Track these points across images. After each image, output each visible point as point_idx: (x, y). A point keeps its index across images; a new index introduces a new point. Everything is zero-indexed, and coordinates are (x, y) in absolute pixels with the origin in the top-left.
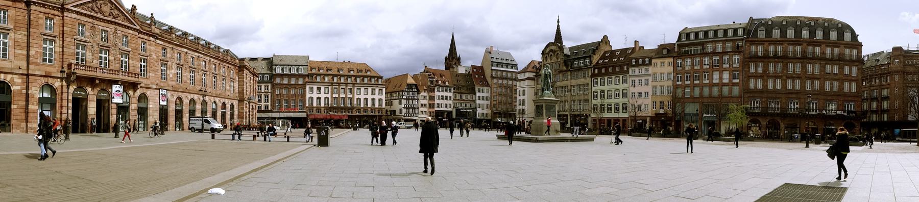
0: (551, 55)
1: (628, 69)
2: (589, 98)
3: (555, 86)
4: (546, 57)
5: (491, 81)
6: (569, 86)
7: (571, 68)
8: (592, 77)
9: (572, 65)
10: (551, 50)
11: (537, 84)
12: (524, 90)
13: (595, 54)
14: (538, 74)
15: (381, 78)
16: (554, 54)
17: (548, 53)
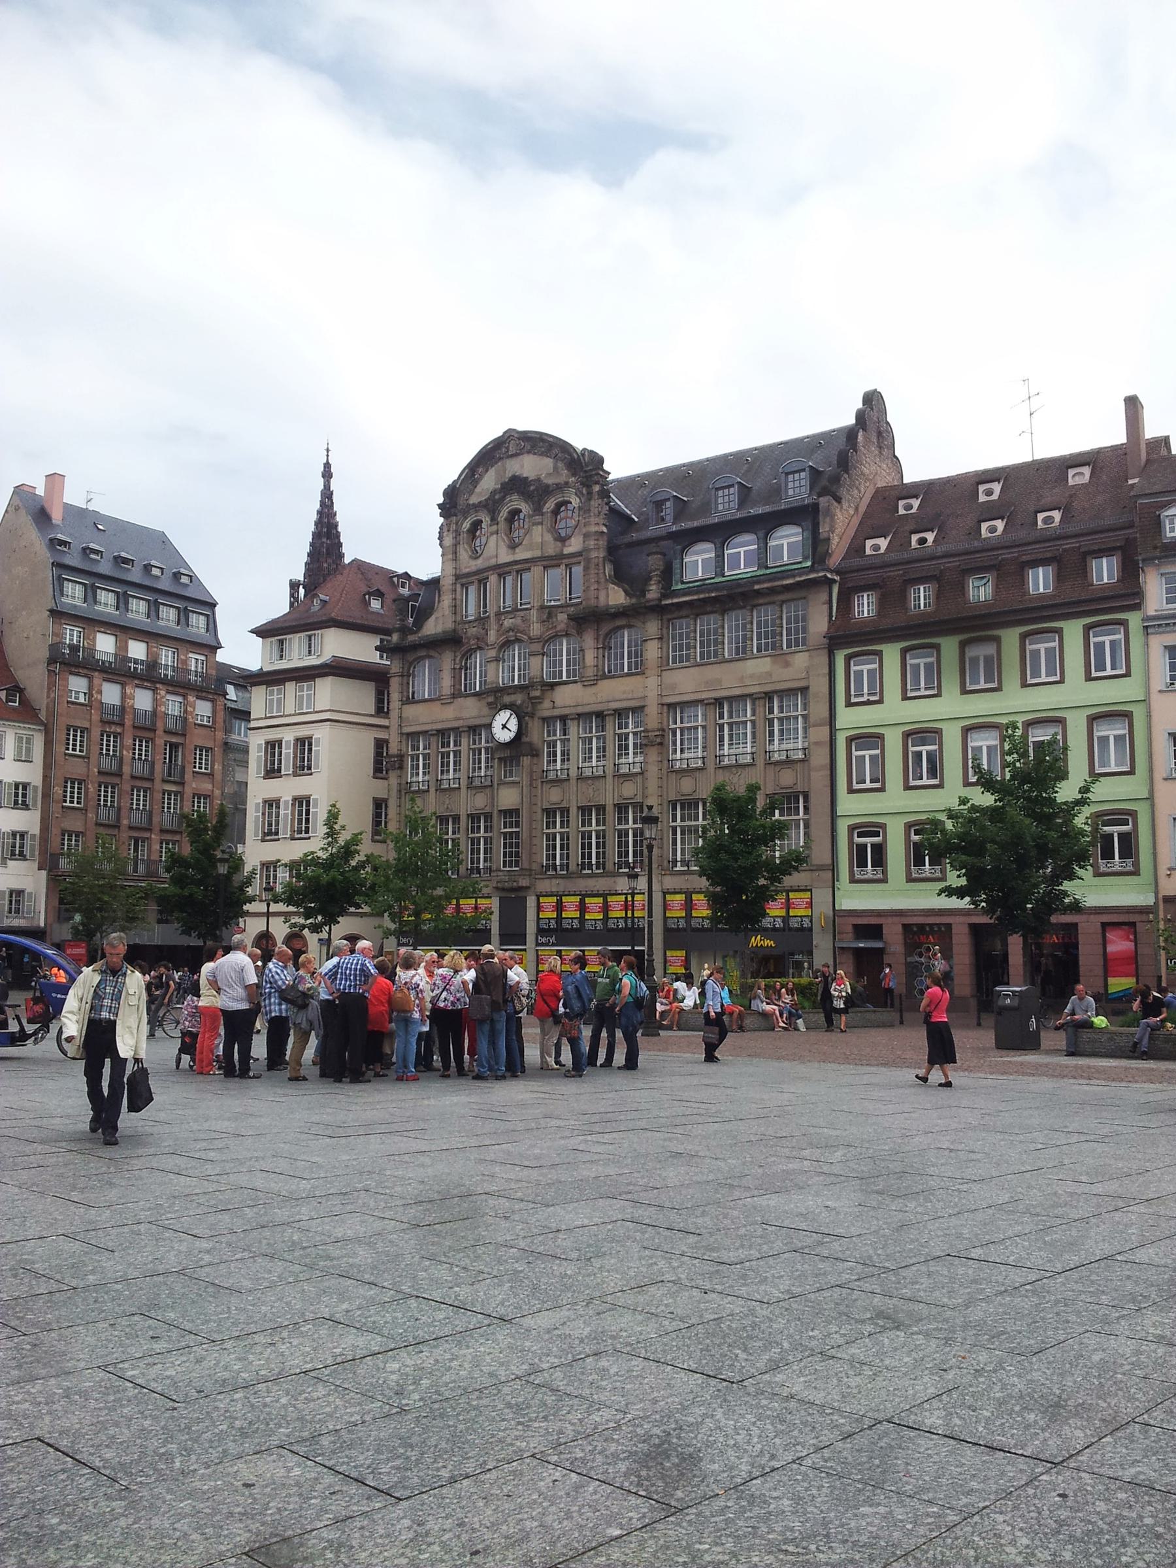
0: (515, 513)
1: (1131, 572)
2: (819, 781)
3: (545, 709)
4: (477, 525)
5: (51, 686)
6: (652, 710)
7: (664, 596)
8: (834, 642)
9: (667, 574)
10: (516, 485)
11: (409, 700)
12: (304, 743)
13: (838, 500)
14: (411, 638)
16: (538, 509)
17: (491, 505)
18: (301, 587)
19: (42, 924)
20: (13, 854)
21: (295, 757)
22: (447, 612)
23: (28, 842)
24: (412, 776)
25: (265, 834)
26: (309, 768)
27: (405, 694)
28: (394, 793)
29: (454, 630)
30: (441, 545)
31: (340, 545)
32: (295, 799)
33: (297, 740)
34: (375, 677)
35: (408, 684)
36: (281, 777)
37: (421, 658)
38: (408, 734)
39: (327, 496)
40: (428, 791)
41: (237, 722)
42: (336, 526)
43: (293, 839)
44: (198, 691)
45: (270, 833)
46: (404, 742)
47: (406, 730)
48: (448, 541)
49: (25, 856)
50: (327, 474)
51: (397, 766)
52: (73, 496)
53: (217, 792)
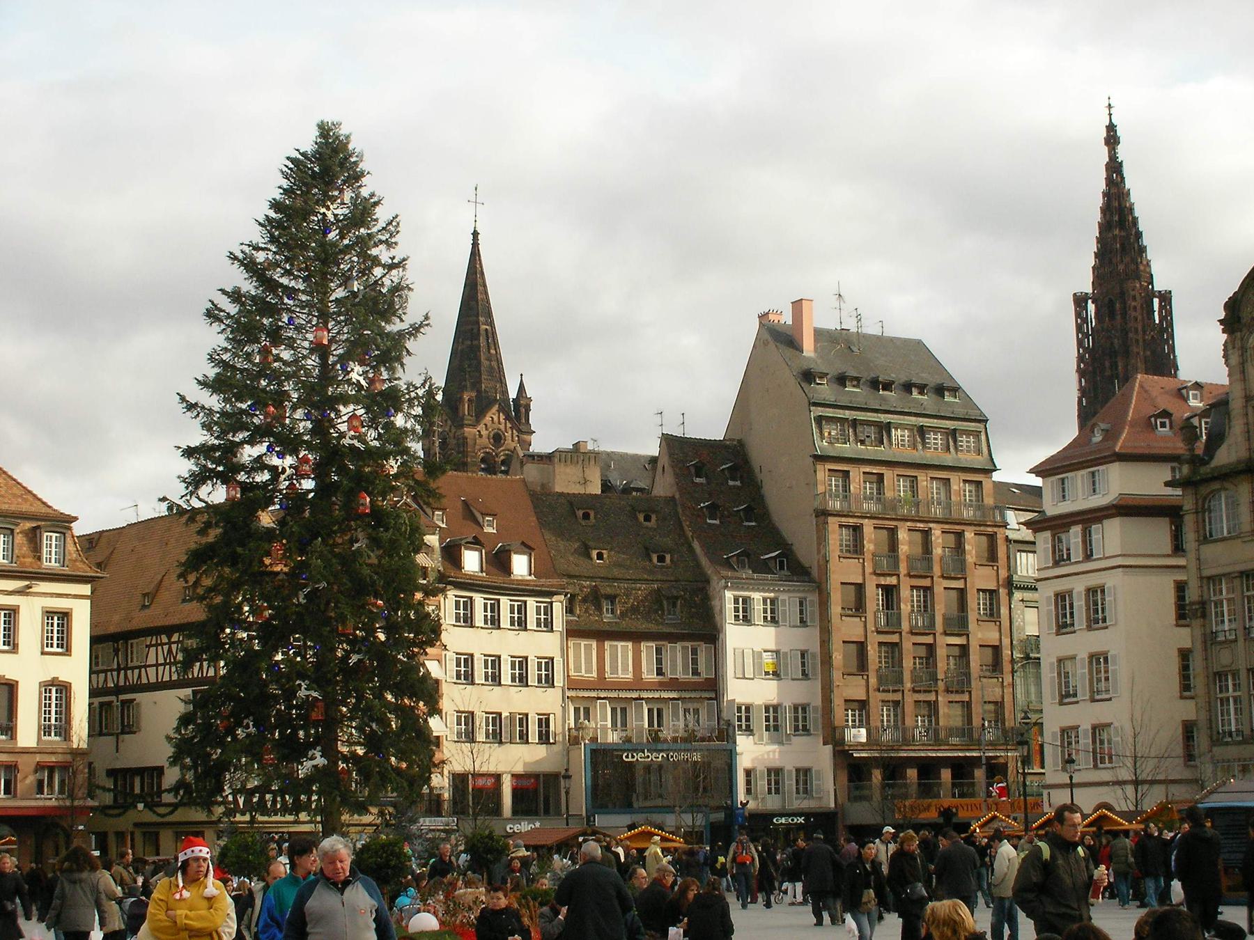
11: (1205, 539)
12: (1094, 593)
15: (62, 523)
18: (1090, 301)
19: (833, 805)
20: (796, 729)
21: (1088, 609)
22: (1240, 439)
23: (811, 715)
24: (1217, 624)
25: (1062, 697)
26: (1104, 620)
27: (1201, 532)
28: (1199, 646)
29: (1250, 459)
30: (1227, 363)
31: (1139, 235)
32: (1091, 656)
33: (1088, 590)
34: (1170, 512)
35: (1204, 521)
36: (1074, 632)
37: (1219, 490)
38: (1209, 578)
39: (1114, 168)
40: (1236, 641)
41: (1024, 555)
42: (1131, 210)
43: (1093, 700)
44: (975, 525)
45: (1068, 695)
46: (1205, 588)
47: (1206, 573)
48: (1235, 359)
49: (808, 730)
50: (1112, 139)
51: (1199, 615)
52: (822, 317)
53: (1006, 641)
